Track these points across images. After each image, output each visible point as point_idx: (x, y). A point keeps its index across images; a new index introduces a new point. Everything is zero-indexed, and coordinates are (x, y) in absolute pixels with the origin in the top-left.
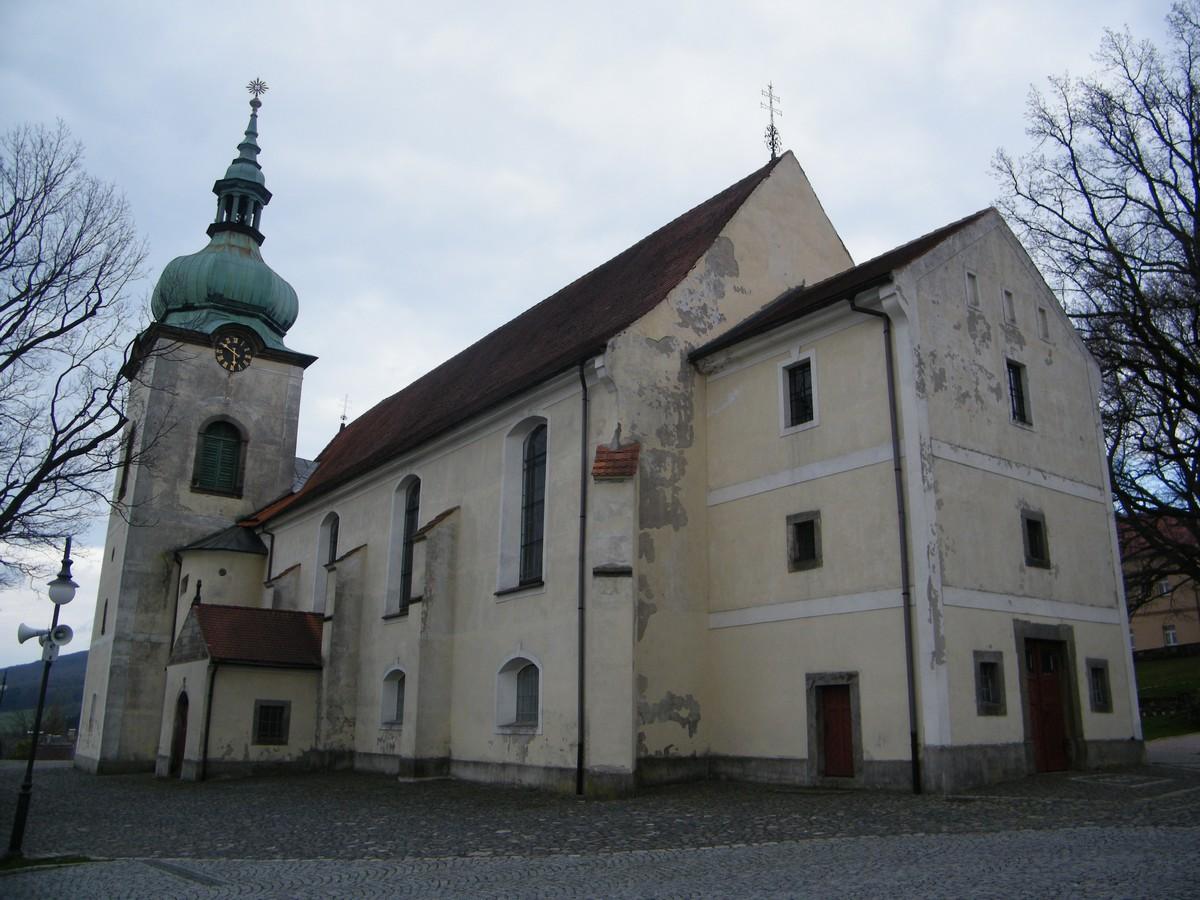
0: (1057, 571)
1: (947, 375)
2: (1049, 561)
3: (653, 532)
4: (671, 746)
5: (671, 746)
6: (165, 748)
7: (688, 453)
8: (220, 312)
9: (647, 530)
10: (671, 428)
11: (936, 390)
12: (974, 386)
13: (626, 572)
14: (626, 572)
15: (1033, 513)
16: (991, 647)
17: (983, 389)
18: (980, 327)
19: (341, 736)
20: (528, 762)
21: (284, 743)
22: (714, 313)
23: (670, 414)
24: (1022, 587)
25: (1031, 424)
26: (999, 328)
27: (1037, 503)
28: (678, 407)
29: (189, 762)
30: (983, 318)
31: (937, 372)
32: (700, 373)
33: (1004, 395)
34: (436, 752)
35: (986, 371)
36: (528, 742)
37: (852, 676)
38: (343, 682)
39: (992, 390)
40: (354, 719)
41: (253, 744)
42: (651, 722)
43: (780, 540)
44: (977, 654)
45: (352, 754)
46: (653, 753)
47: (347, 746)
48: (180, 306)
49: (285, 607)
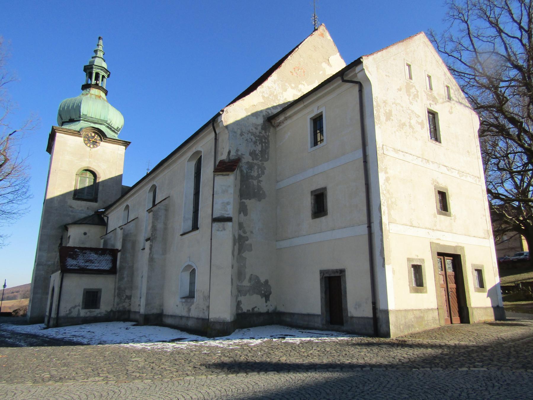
0: (455, 219)
1: (393, 113)
2: (450, 213)
3: (247, 202)
4: (256, 307)
5: (256, 307)
6: (47, 314)
7: (266, 164)
8: (86, 122)
10: (257, 152)
11: (386, 121)
12: (409, 120)
13: (229, 219)
14: (229, 219)
17: (413, 122)
18: (413, 90)
19: (124, 304)
20: (191, 316)
21: (99, 308)
22: (281, 98)
23: (257, 145)
24: (435, 225)
25: (440, 142)
27: (444, 184)
28: (261, 143)
29: (52, 317)
30: (414, 86)
31: (387, 111)
32: (273, 126)
33: (425, 126)
34: (155, 311)
36: (191, 306)
37: (342, 271)
38: (126, 279)
39: (419, 123)
40: (131, 296)
41: (83, 308)
42: (245, 295)
43: (308, 202)
44: (409, 260)
45: (129, 311)
46: (246, 311)
47: (128, 308)
48: (68, 120)
49: (109, 247)
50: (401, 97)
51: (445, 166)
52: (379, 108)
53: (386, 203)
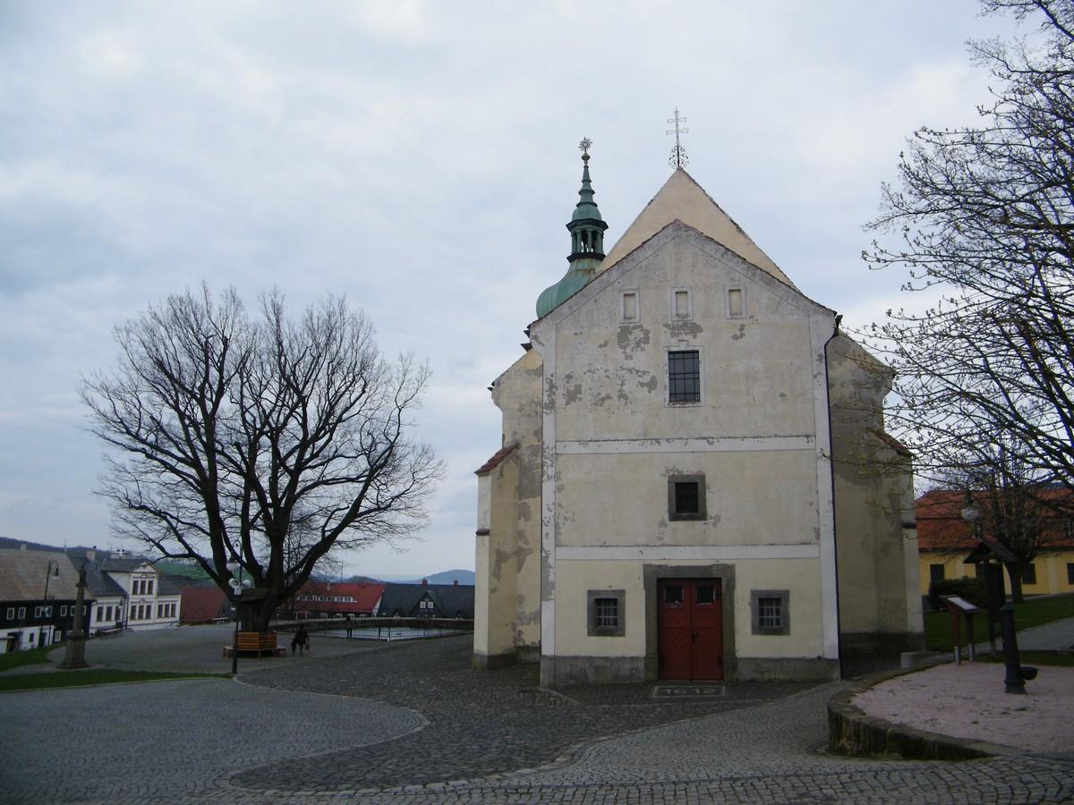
1: (583, 389)
9: (524, 500)
11: (567, 404)
15: (683, 476)
16: (611, 587)
17: (631, 386)
24: (661, 539)
26: (665, 329)
30: (641, 326)
31: (572, 389)
35: (637, 371)
39: (642, 385)
42: (529, 623)
50: (606, 356)
51: (704, 438)
52: (554, 390)
53: (552, 522)
